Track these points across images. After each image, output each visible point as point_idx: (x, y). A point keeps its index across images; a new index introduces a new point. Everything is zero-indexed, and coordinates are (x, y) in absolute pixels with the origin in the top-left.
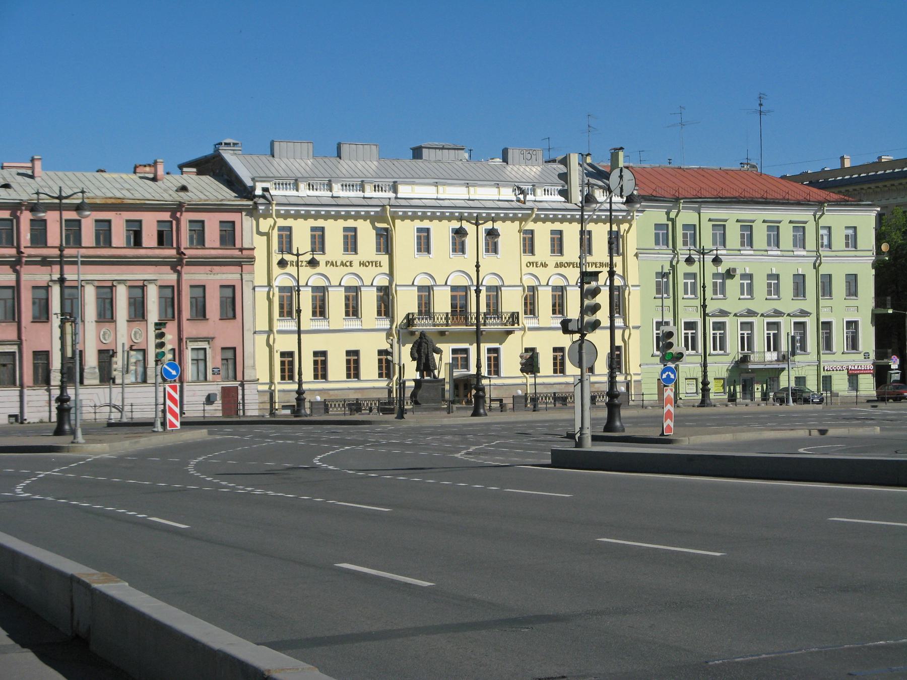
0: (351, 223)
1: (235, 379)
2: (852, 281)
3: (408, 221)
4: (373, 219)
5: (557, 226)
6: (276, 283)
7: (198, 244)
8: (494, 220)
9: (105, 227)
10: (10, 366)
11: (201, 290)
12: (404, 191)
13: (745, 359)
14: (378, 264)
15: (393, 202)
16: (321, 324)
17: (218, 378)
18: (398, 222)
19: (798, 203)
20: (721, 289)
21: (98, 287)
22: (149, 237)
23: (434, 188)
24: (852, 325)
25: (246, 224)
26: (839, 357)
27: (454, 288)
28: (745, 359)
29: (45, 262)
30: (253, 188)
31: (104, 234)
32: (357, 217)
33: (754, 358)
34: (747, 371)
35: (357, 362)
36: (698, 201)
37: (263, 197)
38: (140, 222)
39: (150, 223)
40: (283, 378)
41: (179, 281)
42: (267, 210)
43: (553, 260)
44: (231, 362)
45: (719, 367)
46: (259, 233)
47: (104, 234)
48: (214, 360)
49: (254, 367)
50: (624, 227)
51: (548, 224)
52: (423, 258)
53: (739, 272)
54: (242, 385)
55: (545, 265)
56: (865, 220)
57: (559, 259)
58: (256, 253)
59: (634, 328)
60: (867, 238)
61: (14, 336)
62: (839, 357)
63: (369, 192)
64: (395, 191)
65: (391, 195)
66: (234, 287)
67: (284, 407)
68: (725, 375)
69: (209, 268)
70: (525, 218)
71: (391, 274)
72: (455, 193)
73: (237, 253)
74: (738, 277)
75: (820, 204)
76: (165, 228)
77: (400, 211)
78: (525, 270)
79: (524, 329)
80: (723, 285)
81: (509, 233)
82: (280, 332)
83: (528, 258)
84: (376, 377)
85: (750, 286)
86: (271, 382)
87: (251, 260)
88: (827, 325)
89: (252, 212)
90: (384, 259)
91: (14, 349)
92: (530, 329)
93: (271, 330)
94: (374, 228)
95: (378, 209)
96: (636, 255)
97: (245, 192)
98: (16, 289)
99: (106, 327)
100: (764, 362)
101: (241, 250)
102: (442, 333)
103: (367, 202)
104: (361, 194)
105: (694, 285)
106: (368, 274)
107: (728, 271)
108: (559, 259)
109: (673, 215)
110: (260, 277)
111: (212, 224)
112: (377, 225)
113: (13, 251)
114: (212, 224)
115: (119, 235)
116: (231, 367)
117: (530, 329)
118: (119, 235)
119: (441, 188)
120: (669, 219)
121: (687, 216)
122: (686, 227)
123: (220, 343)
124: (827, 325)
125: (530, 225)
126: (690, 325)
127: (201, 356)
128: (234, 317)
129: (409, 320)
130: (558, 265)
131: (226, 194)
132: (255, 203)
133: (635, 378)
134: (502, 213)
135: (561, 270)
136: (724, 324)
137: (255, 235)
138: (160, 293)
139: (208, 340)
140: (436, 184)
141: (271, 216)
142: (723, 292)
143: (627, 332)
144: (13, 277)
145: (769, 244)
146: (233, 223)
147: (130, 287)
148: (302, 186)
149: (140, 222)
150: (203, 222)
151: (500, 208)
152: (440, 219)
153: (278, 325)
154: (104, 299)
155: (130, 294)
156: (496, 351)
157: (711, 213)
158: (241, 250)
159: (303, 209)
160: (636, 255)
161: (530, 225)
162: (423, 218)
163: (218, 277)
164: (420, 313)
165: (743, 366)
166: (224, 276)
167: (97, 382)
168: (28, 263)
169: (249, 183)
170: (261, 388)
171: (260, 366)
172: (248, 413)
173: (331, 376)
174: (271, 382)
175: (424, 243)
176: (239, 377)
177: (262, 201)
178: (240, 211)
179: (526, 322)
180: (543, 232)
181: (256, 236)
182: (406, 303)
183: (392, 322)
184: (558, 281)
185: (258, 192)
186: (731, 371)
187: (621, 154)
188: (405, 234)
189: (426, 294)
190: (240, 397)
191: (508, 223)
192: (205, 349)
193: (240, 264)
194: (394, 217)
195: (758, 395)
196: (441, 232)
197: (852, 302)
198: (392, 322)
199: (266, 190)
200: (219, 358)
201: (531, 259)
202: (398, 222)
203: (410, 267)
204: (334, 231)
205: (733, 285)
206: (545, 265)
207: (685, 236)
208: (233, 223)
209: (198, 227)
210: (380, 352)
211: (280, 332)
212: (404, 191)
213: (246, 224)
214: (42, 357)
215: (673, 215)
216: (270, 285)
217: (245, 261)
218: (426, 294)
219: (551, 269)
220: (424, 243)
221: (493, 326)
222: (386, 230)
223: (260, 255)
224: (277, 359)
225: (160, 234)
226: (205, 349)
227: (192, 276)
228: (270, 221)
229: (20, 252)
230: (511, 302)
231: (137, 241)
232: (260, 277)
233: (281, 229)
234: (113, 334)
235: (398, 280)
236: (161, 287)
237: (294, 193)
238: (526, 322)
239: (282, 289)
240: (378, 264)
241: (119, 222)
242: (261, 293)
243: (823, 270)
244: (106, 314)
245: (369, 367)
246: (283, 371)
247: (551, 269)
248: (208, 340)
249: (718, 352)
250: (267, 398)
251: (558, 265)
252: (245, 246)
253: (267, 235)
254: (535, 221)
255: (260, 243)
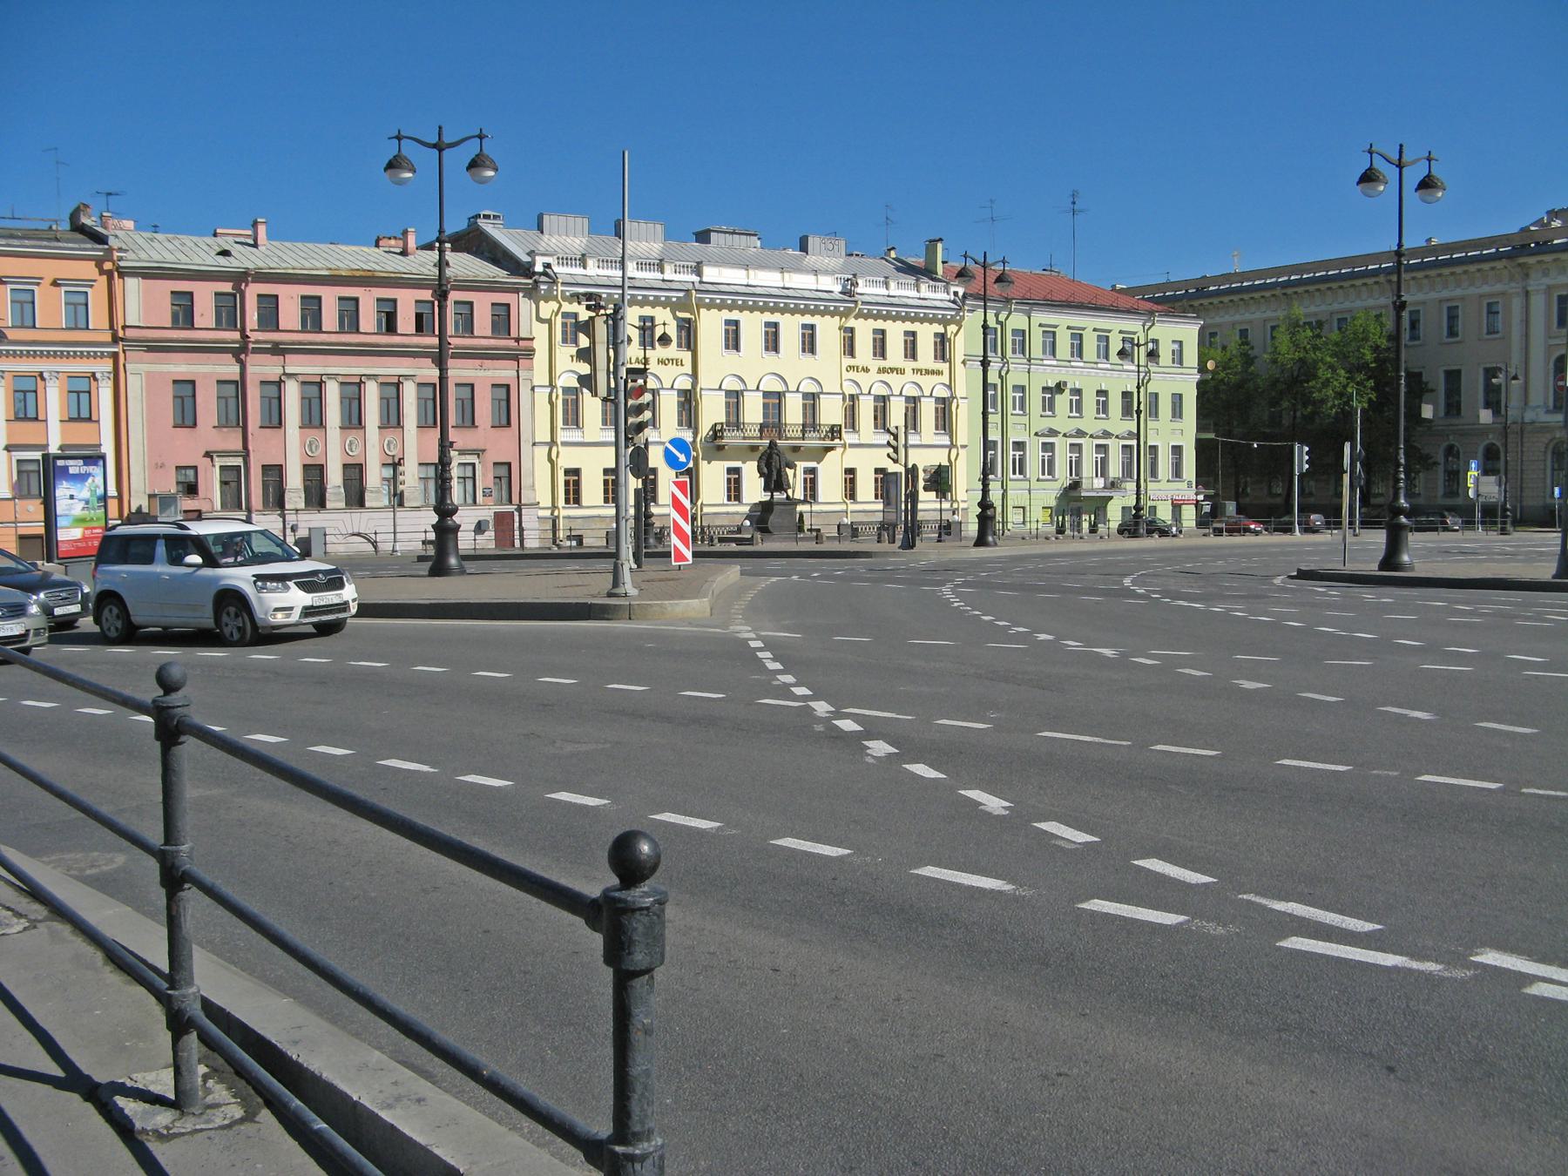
0: (808, 319)
1: (510, 501)
2: (1178, 400)
3: (714, 311)
4: (674, 307)
5: (880, 324)
6: (560, 383)
7: (464, 330)
8: (813, 313)
9: (350, 306)
10: (233, 485)
11: (468, 389)
12: (710, 274)
13: (1075, 485)
14: (939, 373)
15: (697, 286)
16: (574, 436)
17: (490, 500)
18: (703, 311)
19: (1128, 312)
20: (1049, 405)
21: (342, 383)
22: (405, 322)
23: (744, 272)
24: (1177, 450)
25: (524, 308)
26: (1163, 485)
27: (766, 394)
28: (1075, 485)
29: (277, 350)
30: (532, 264)
31: (350, 314)
32: (655, 303)
33: (1085, 484)
34: (1079, 499)
35: (577, 484)
36: (1030, 303)
37: (545, 274)
38: (395, 301)
39: (407, 303)
40: (567, 501)
41: (443, 378)
42: (550, 291)
43: (876, 364)
44: (505, 481)
45: (1048, 494)
46: (539, 319)
47: (350, 314)
48: (485, 478)
49: (533, 487)
50: (952, 328)
51: (871, 321)
52: (808, 357)
53: (1069, 386)
54: (519, 510)
55: (866, 370)
56: (1188, 332)
57: (883, 364)
58: (535, 344)
59: (964, 447)
60: (1191, 356)
61: (239, 446)
62: (1163, 485)
63: (669, 274)
64: (699, 273)
65: (695, 278)
66: (508, 386)
67: (569, 538)
68: (1053, 503)
69: (478, 362)
70: (845, 314)
71: (694, 375)
72: (768, 279)
73: (512, 343)
74: (1067, 391)
75: (1151, 313)
76: (425, 310)
77: (707, 298)
78: (846, 375)
79: (844, 446)
80: (1052, 401)
81: (829, 331)
82: (565, 444)
83: (848, 361)
84: (601, 502)
85: (1079, 403)
86: (554, 507)
87: (530, 353)
88: (1154, 449)
89: (532, 293)
90: (686, 356)
91: (239, 461)
92: (852, 446)
93: (553, 443)
94: (675, 317)
95: (681, 294)
96: (964, 362)
97: (526, 270)
98: (240, 384)
99: (353, 435)
100: (1092, 490)
101: (517, 340)
102: (796, 449)
103: (667, 285)
104: (658, 275)
105: (1022, 399)
106: (927, 382)
107: (1058, 385)
108: (883, 364)
109: (1002, 317)
110: (540, 375)
111: (483, 305)
112: (680, 315)
113: (236, 335)
114: (483, 305)
115: (369, 318)
116: (505, 487)
117: (852, 446)
118: (369, 318)
119: (751, 272)
120: (998, 322)
121: (1017, 321)
122: (1015, 332)
123: (494, 456)
124: (1154, 449)
125: (851, 323)
126: (1019, 446)
127: (470, 474)
128: (509, 424)
129: (716, 433)
130: (882, 371)
131: (499, 274)
132: (536, 282)
133: (962, 505)
134: (740, 300)
135: (885, 377)
136: (1052, 444)
137: (536, 321)
138: (418, 392)
139: (478, 453)
140: (782, 270)
141: (555, 298)
142: (1052, 408)
143: (954, 452)
144: (237, 369)
145: (1044, 352)
146: (508, 305)
147: (304, 383)
148: (590, 262)
149: (395, 301)
150: (471, 304)
151: (892, 305)
152: (752, 309)
153: (562, 436)
154: (270, 399)
155: (302, 392)
156: (813, 471)
157: (1041, 317)
158: (517, 340)
159: (729, 299)
160: (964, 362)
161: (851, 323)
162: (732, 307)
163: (489, 373)
164: (728, 424)
165: (1074, 494)
166: (498, 373)
167: (343, 505)
168: (256, 351)
169: (525, 259)
170: (542, 513)
171: (539, 486)
172: (528, 544)
173: (586, 498)
174: (554, 507)
175: (733, 339)
176: (515, 499)
177: (543, 279)
178: (517, 291)
179: (848, 437)
180: (864, 331)
181: (535, 324)
182: (712, 411)
183: (695, 434)
184: (911, 391)
185: (539, 268)
186: (1059, 499)
187: (940, 246)
188: (710, 325)
189: (734, 399)
190: (517, 525)
191: (828, 317)
192: (473, 465)
193: (516, 358)
194: (701, 304)
195: (1085, 525)
196: (752, 326)
197: (1177, 425)
198: (695, 434)
199: (548, 266)
200: (491, 476)
201: (852, 362)
202: (703, 311)
203: (753, 367)
204: (790, 327)
205: (1062, 401)
206: (866, 370)
207: (1014, 342)
208: (508, 305)
209: (465, 310)
210: (606, 472)
211: (565, 444)
212: (710, 274)
213: (524, 308)
214: (274, 473)
215: (1002, 317)
216: (552, 385)
217: (521, 354)
218: (734, 399)
219: (873, 376)
220: (733, 339)
221: (813, 441)
222: (688, 321)
223: (540, 346)
224: (561, 478)
225: (419, 317)
226: (473, 465)
227: (458, 371)
228: (553, 305)
229: (244, 336)
230: (832, 412)
231: (390, 325)
232: (540, 375)
233: (565, 315)
234: (361, 444)
235: (703, 382)
236: (419, 385)
237: (579, 271)
238: (848, 437)
239: (566, 390)
240: (939, 373)
241: (369, 299)
242: (542, 395)
243: (1152, 388)
244: (313, 418)
245: (592, 490)
246: (567, 492)
247: (873, 376)
248: (478, 453)
249: (1018, 476)
250: (549, 526)
251: (882, 371)
252: (522, 335)
253: (549, 321)
254: (856, 318)
255: (540, 332)
